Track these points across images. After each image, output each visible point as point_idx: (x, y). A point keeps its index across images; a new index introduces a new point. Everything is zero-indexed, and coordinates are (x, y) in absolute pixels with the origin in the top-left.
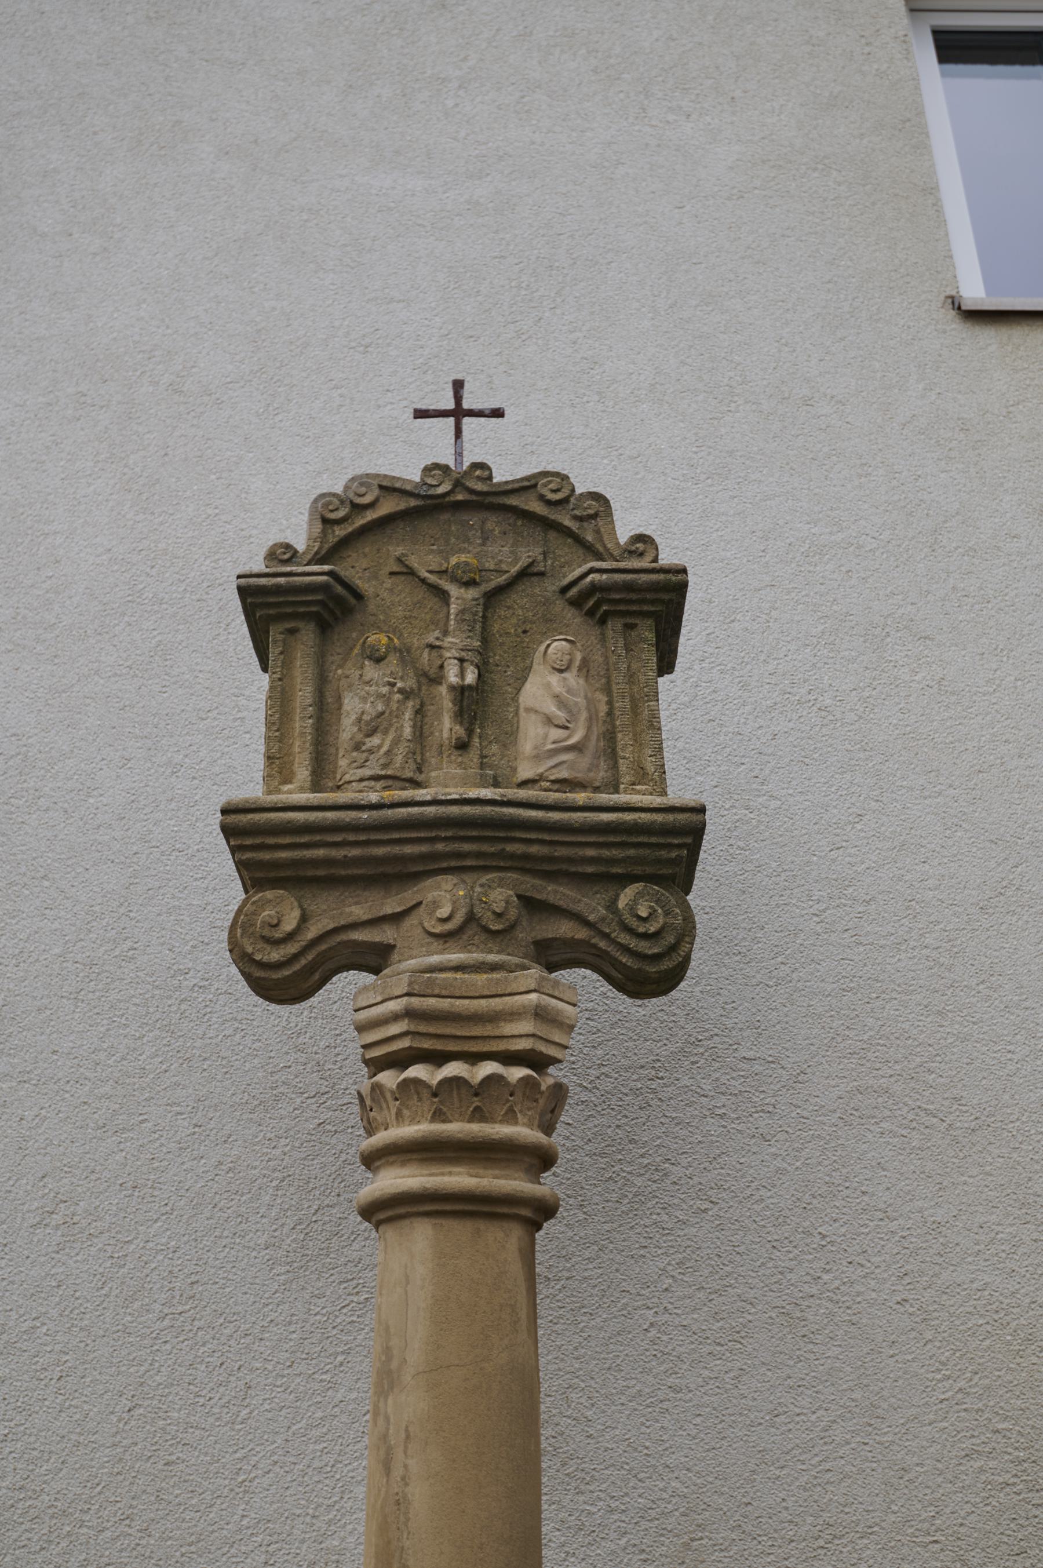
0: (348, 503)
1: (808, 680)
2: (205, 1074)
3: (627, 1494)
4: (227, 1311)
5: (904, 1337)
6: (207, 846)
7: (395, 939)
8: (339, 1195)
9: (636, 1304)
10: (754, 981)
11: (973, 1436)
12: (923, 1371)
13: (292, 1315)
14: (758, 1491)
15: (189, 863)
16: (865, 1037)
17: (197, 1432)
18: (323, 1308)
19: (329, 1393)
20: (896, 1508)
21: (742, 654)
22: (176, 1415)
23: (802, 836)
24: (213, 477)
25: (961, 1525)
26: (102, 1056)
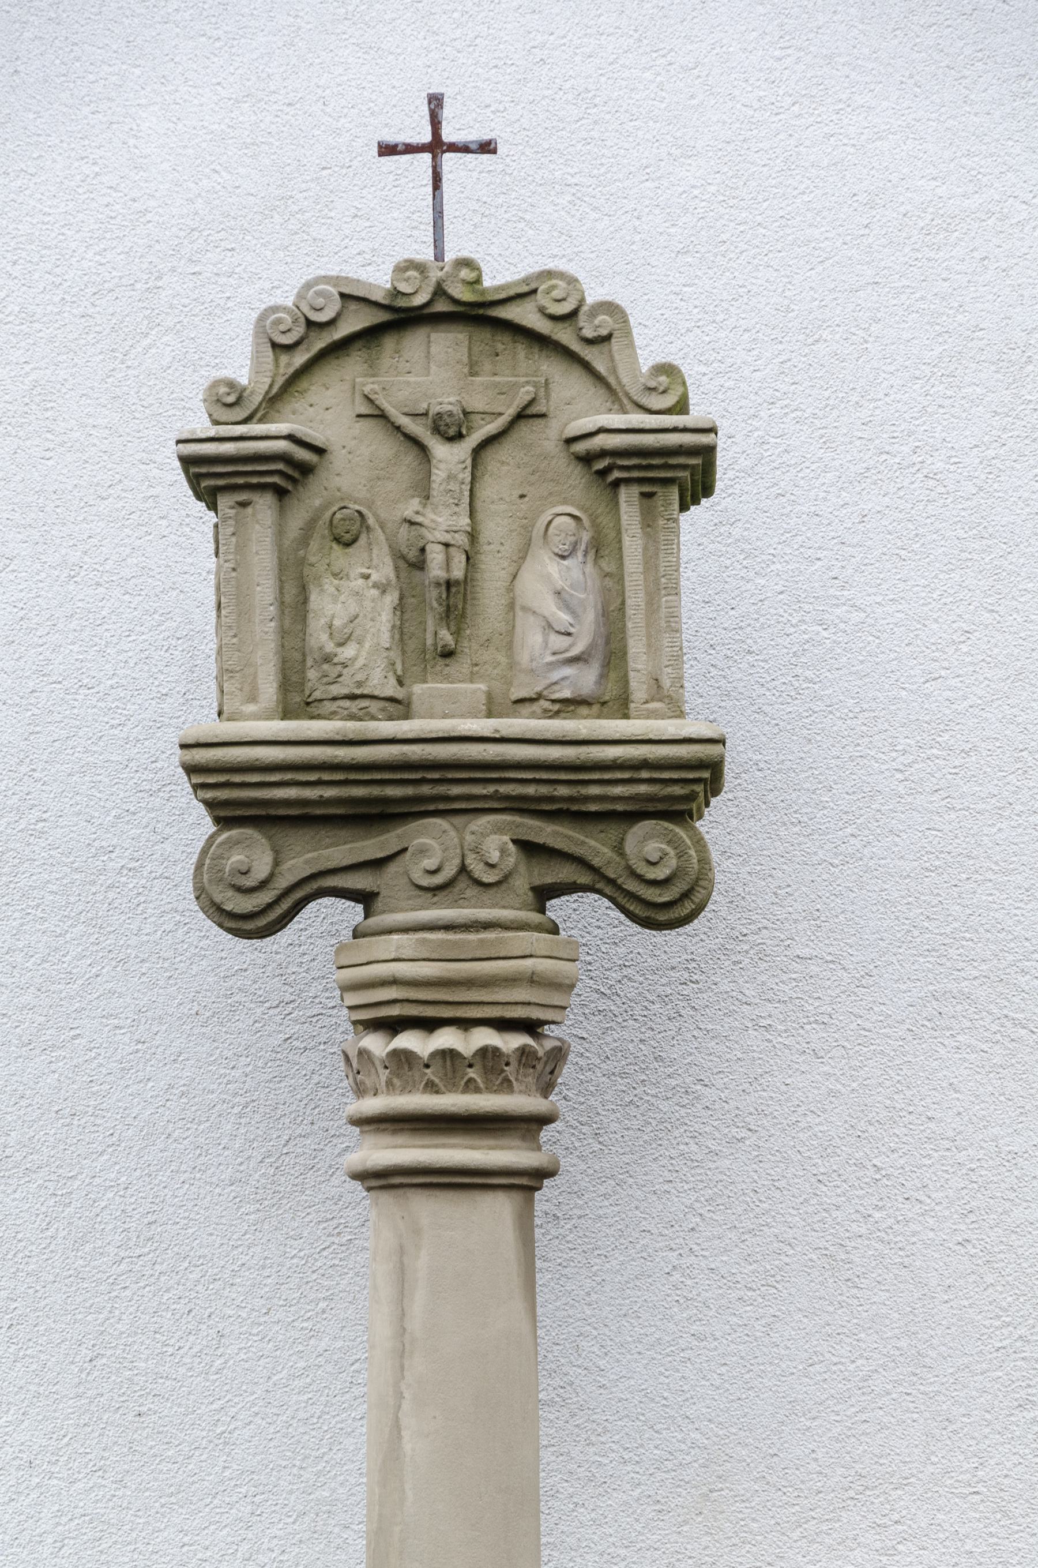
0: (302, 320)
1: (913, 433)
2: (144, 979)
3: (642, 1446)
4: (192, 1253)
5: (962, 1282)
6: (124, 682)
7: (378, 886)
8: (312, 1123)
9: (658, 1245)
10: (815, 859)
11: (1029, 1386)
12: (979, 1317)
13: (266, 1258)
14: (786, 1442)
15: (102, 704)
16: (948, 930)
17: (168, 1383)
18: (300, 1250)
19: (312, 1342)
20: (936, 1460)
21: (827, 394)
22: (143, 1365)
23: (889, 662)
24: (86, 110)
25: (1006, 1476)
26: (19, 957)
